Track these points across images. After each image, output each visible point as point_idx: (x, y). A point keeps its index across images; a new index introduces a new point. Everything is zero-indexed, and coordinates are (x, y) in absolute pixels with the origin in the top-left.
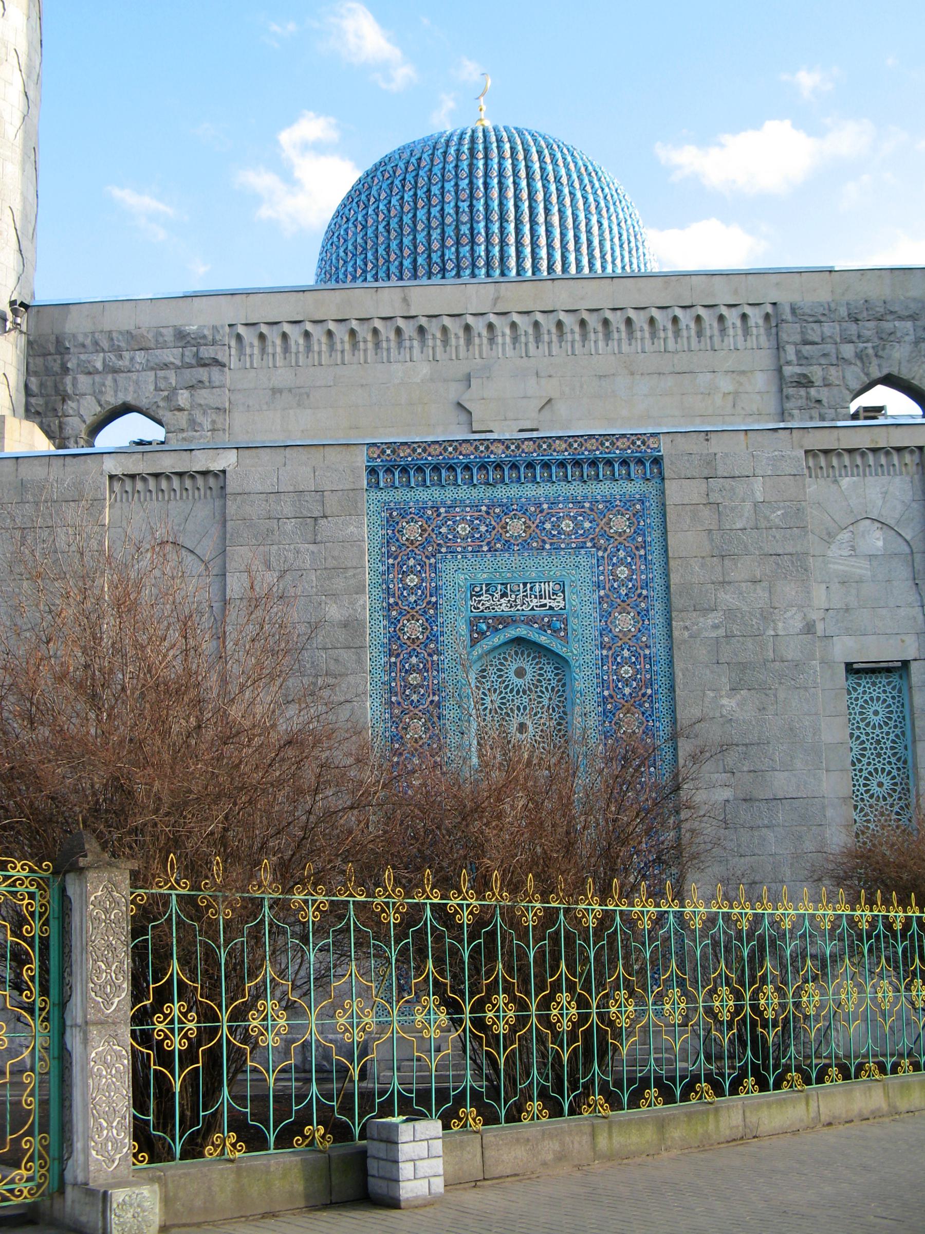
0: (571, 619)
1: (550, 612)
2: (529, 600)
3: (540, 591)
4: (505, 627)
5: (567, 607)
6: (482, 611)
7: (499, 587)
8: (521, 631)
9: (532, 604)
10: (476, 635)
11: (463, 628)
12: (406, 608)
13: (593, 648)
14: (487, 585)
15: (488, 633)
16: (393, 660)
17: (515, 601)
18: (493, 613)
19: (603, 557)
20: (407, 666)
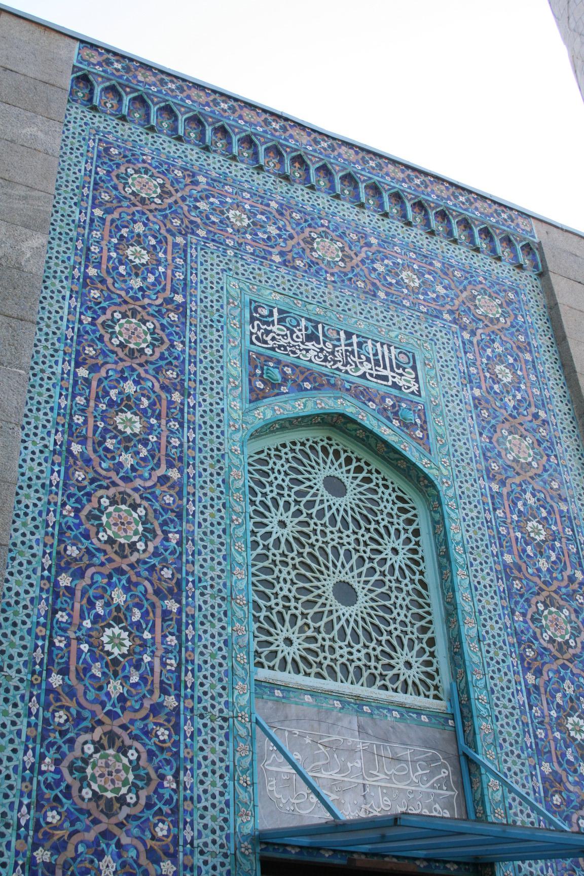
0: (430, 416)
1: (395, 392)
2: (356, 359)
3: (376, 354)
4: (315, 388)
5: (423, 393)
6: (273, 349)
7: (303, 323)
8: (348, 406)
11: (235, 368)
12: (123, 293)
13: (475, 474)
14: (280, 312)
15: (284, 389)
16: (83, 372)
17: (332, 353)
18: (291, 358)
19: (471, 342)
20: (113, 393)
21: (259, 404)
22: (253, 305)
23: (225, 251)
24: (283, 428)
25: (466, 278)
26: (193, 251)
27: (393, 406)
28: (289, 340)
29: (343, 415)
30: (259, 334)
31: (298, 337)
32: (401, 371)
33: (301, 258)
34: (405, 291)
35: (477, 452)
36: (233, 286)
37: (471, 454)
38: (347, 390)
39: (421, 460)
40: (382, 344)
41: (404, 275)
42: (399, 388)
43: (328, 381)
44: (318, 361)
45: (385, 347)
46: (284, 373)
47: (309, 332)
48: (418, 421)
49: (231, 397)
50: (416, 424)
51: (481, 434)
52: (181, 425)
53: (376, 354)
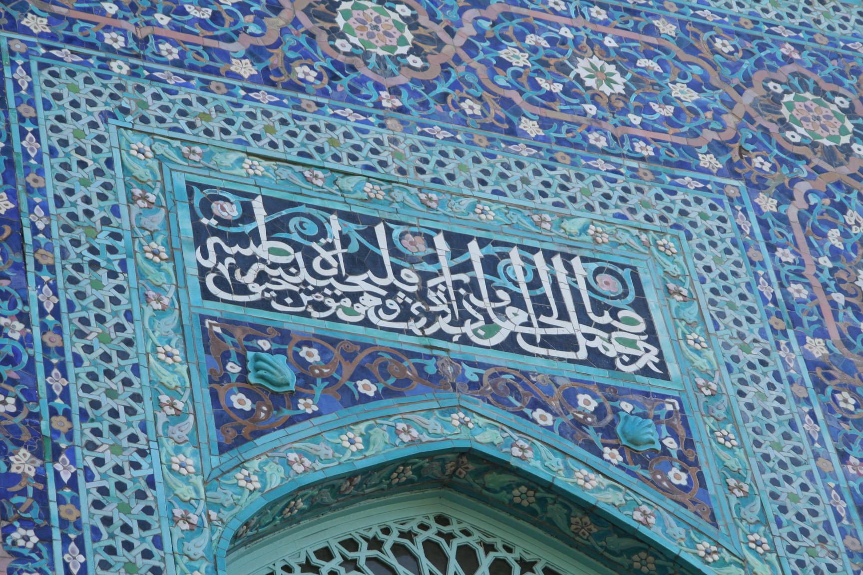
0: (701, 427)
1: (598, 375)
2: (486, 304)
3: (534, 284)
4: (387, 393)
5: (673, 369)
6: (264, 304)
7: (335, 226)
8: (482, 430)
9: (505, 329)
10: (241, 402)
11: (171, 365)
14: (271, 205)
15: (306, 405)
17: (421, 295)
18: (315, 323)
19: (783, 219)
21: (246, 451)
22: (198, 196)
23: (104, 63)
24: (316, 508)
25: (748, 54)
26: (20, 73)
27: (600, 412)
28: (304, 274)
29: (469, 454)
30: (224, 269)
31: (325, 265)
32: (606, 319)
33: (307, 58)
34: (591, 109)
35: (841, 506)
36: (136, 153)
37: (825, 513)
38: (473, 386)
39: (693, 544)
40: (548, 256)
41: (582, 68)
42: (609, 364)
43: (420, 368)
44: (385, 320)
45: (557, 260)
46: (302, 363)
47: (354, 248)
48: (671, 444)
49: (169, 445)
50: (665, 451)
51: (844, 457)
52: (45, 535)
53: (534, 284)
